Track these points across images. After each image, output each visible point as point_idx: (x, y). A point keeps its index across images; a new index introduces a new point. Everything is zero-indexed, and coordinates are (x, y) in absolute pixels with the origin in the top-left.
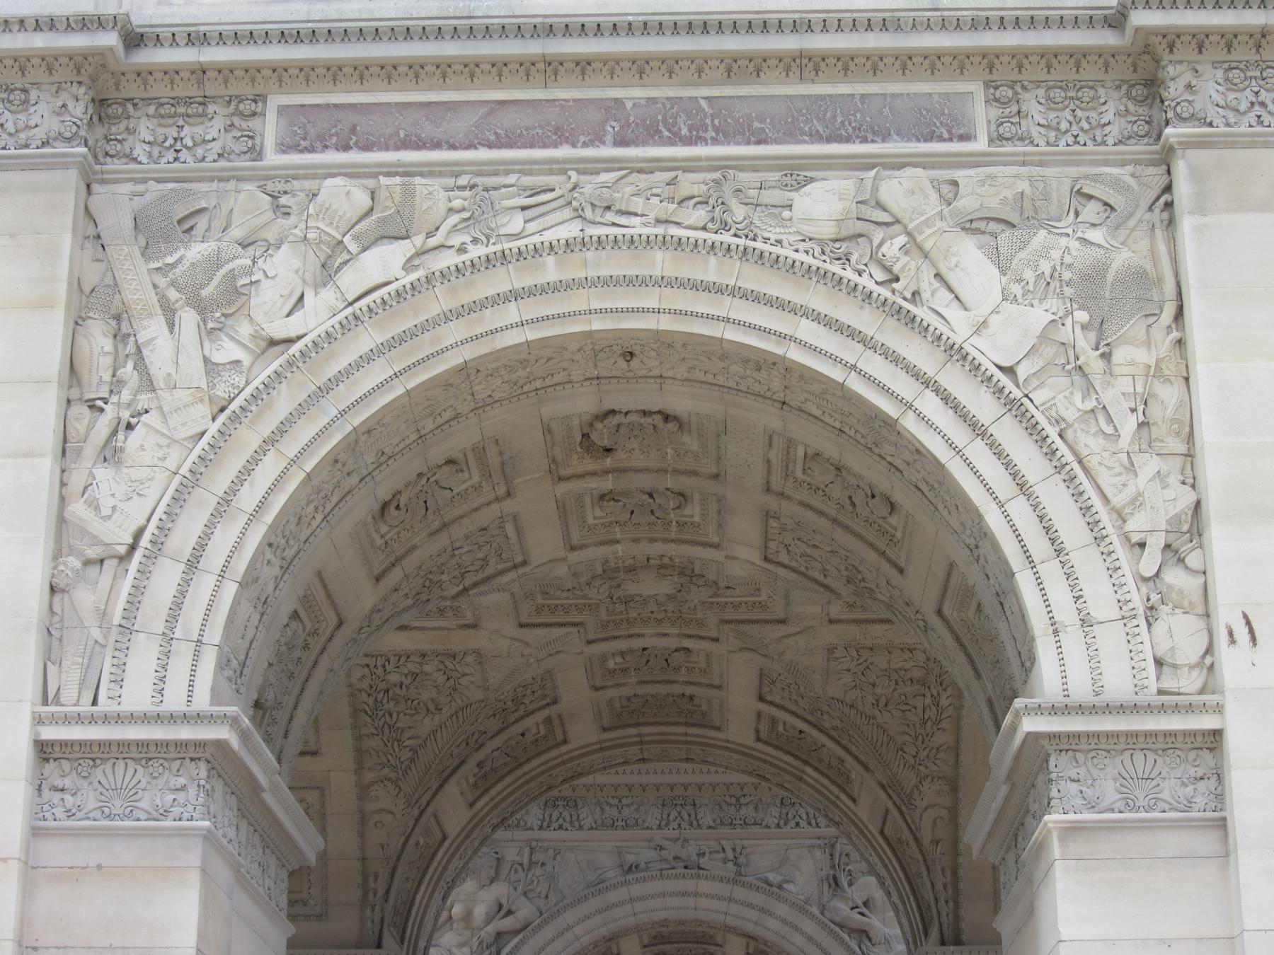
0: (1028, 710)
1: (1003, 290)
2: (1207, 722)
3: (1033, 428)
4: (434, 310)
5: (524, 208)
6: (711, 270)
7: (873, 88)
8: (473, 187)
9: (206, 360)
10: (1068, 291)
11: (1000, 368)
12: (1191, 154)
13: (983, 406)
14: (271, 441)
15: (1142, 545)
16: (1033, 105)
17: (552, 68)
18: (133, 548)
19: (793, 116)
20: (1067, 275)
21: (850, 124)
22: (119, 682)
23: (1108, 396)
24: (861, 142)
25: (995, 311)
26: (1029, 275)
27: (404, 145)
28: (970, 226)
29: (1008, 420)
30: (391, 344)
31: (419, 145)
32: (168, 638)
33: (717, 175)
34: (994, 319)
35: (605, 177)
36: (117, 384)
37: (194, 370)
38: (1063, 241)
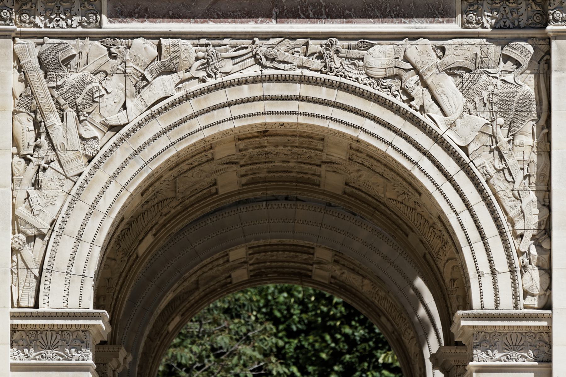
1: (464, 106)
4: (190, 112)
5: (233, 58)
6: (323, 93)
8: (207, 45)
9: (81, 137)
10: (495, 108)
11: (460, 147)
14: (113, 177)
15: (522, 236)
19: (365, 8)
20: (495, 100)
21: (393, 13)
23: (510, 162)
24: (398, 23)
25: (461, 117)
26: (477, 99)
29: (462, 173)
30: (169, 129)
35: (272, 41)
36: (37, 147)
38: (494, 80)
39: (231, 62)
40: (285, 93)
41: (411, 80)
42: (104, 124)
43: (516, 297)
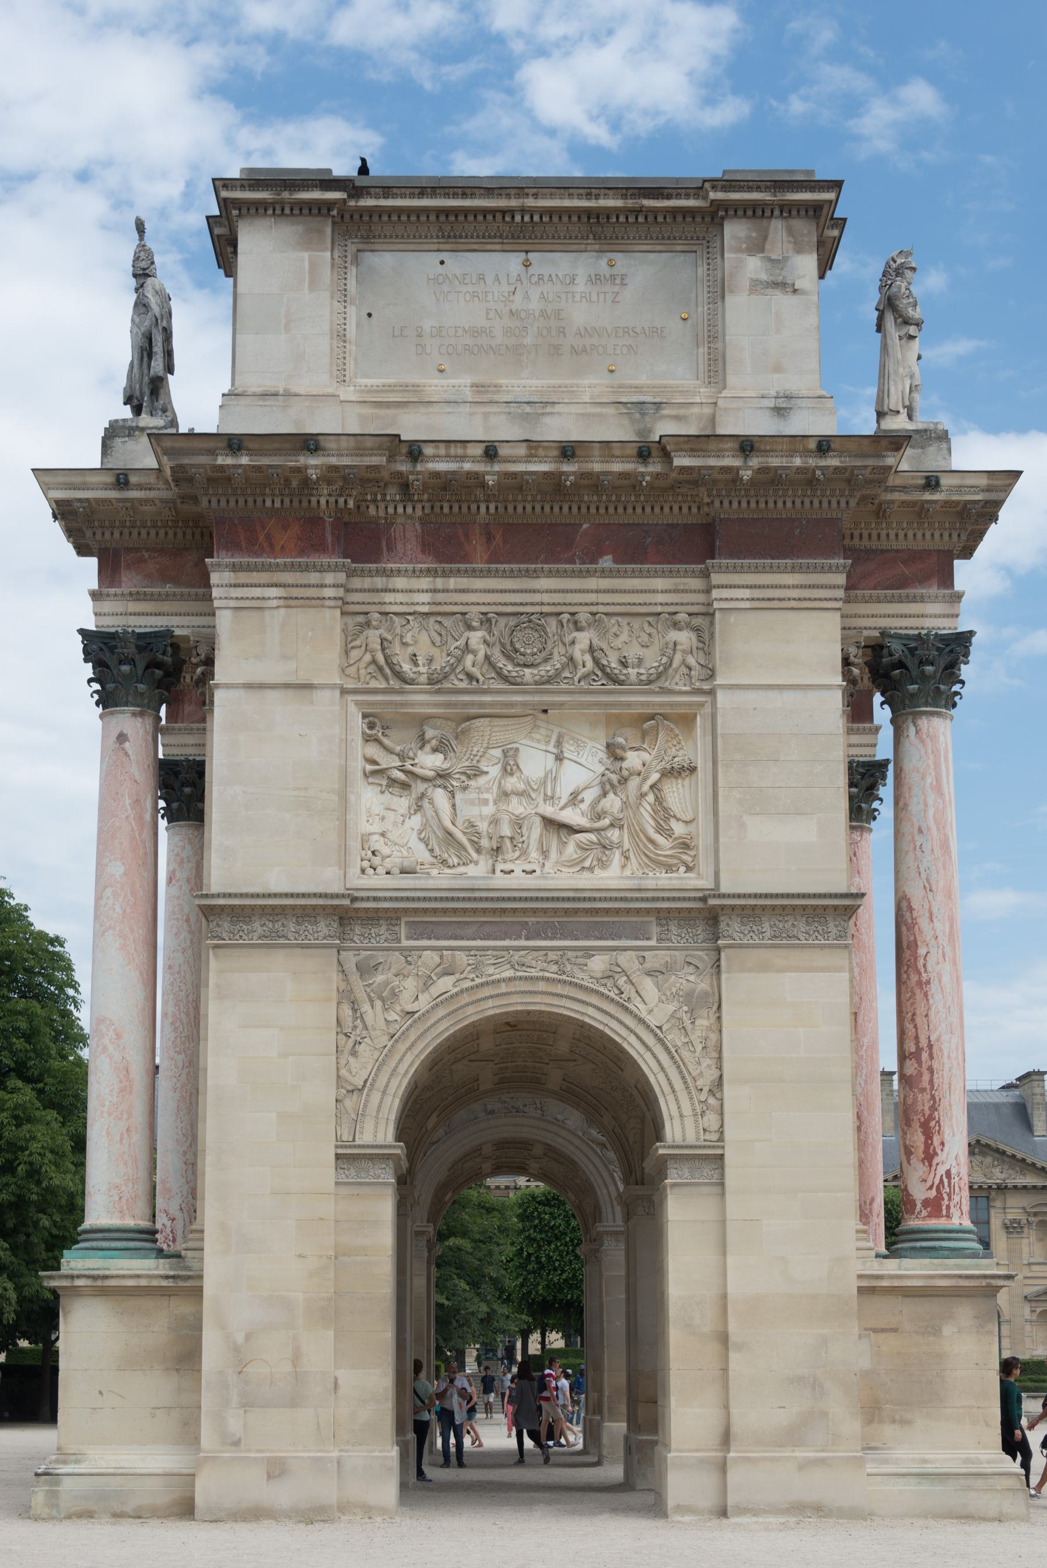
0: (661, 1147)
2: (719, 1152)
3: (667, 1049)
4: (464, 1002)
6: (559, 989)
7: (617, 919)
10: (681, 999)
12: (727, 950)
13: (650, 1040)
14: (409, 1049)
16: (674, 929)
17: (504, 911)
18: (364, 1086)
20: (681, 993)
22: (362, 1133)
23: (693, 1037)
25: (656, 1006)
26: (668, 993)
27: (450, 938)
28: (649, 974)
30: (449, 1014)
31: (456, 938)
32: (377, 1117)
33: (561, 953)
34: (655, 1009)
35: (522, 953)
37: (382, 1024)
39: (493, 967)
40: (531, 989)
41: (622, 981)
42: (402, 1011)
43: (697, 1133)
